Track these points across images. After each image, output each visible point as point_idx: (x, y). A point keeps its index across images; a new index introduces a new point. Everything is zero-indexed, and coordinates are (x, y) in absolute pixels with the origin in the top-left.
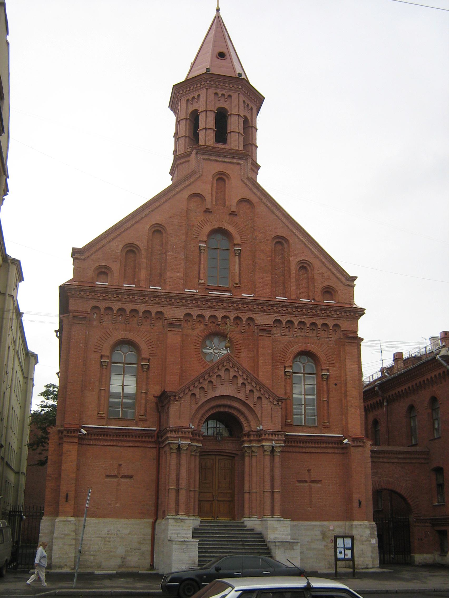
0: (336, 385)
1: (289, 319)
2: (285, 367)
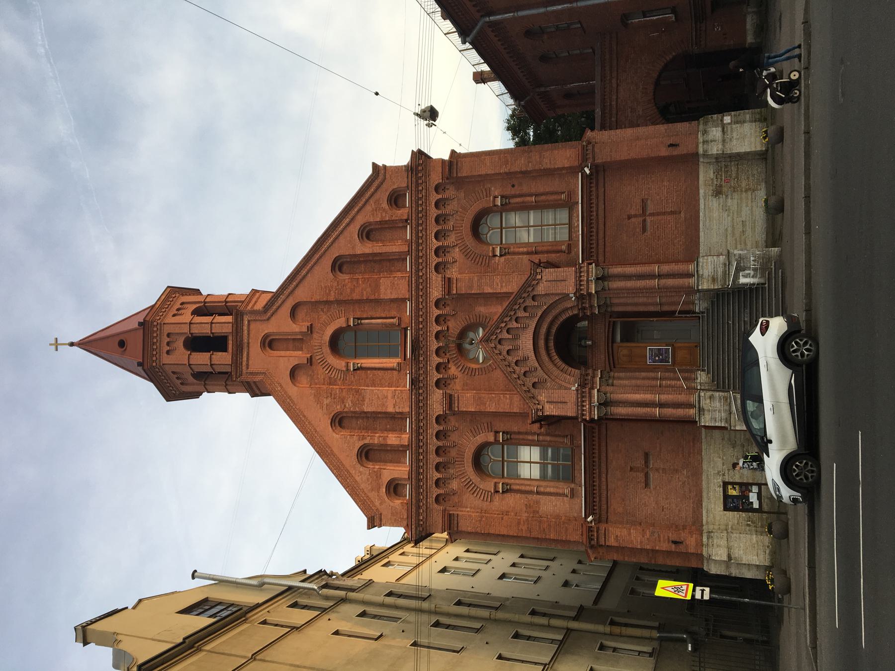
0: (513, 186)
2: (495, 256)
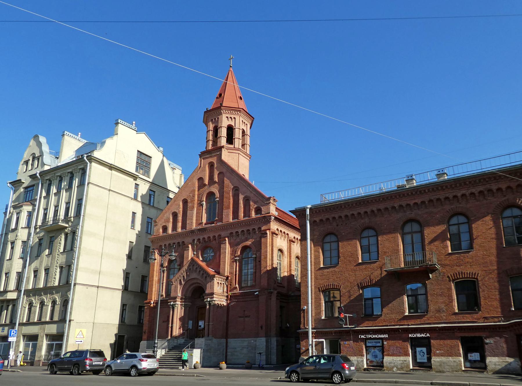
1: (237, 230)
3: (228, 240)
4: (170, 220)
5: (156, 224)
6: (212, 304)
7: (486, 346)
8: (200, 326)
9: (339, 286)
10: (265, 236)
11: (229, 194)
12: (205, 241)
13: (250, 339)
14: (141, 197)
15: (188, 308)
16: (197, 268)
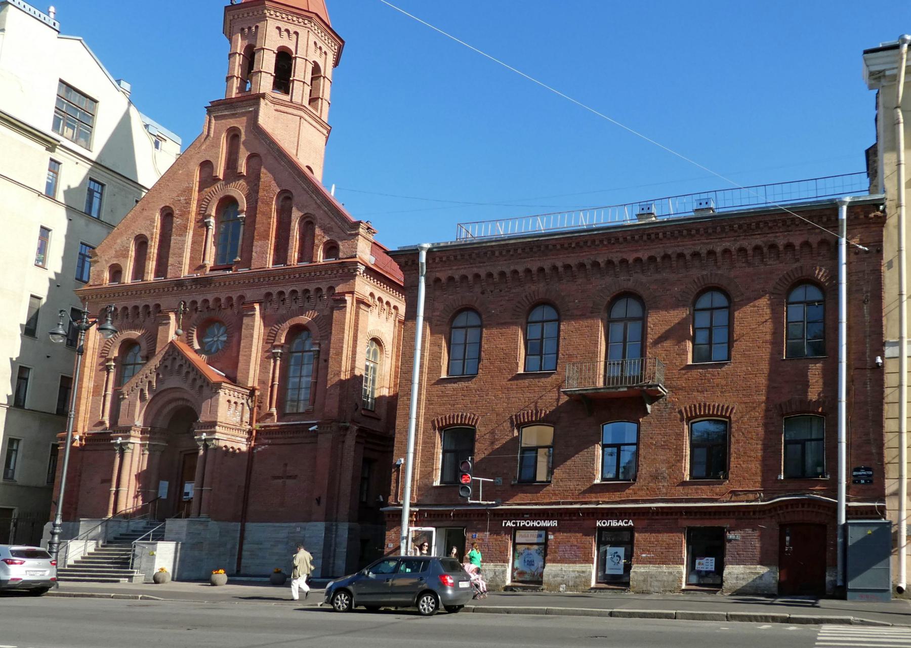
1: (280, 289)
3: (260, 309)
4: (128, 252)
5: (96, 258)
6: (212, 447)
7: (728, 545)
8: (187, 494)
9: (473, 419)
10: (342, 305)
11: (269, 204)
12: (208, 308)
13: (294, 524)
14: (65, 192)
15: (158, 453)
16: (181, 366)
